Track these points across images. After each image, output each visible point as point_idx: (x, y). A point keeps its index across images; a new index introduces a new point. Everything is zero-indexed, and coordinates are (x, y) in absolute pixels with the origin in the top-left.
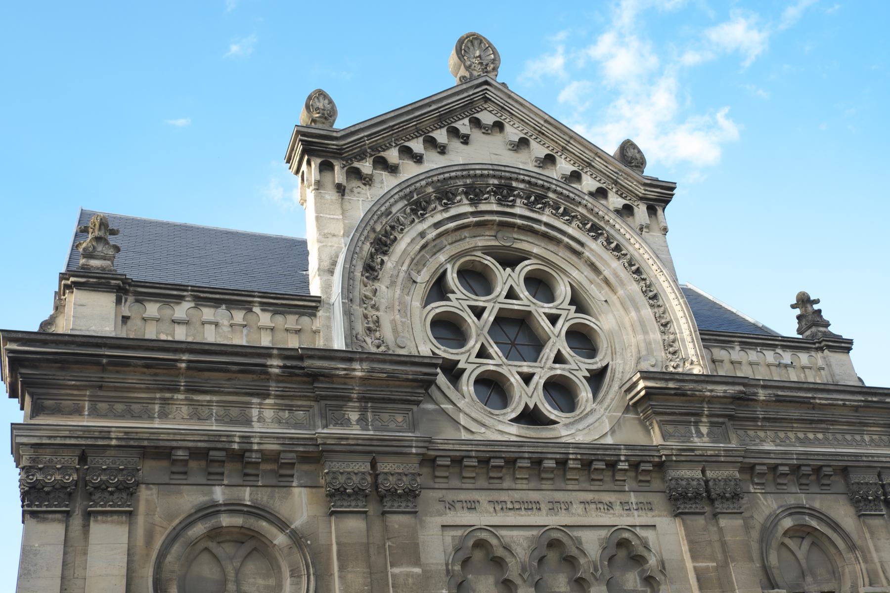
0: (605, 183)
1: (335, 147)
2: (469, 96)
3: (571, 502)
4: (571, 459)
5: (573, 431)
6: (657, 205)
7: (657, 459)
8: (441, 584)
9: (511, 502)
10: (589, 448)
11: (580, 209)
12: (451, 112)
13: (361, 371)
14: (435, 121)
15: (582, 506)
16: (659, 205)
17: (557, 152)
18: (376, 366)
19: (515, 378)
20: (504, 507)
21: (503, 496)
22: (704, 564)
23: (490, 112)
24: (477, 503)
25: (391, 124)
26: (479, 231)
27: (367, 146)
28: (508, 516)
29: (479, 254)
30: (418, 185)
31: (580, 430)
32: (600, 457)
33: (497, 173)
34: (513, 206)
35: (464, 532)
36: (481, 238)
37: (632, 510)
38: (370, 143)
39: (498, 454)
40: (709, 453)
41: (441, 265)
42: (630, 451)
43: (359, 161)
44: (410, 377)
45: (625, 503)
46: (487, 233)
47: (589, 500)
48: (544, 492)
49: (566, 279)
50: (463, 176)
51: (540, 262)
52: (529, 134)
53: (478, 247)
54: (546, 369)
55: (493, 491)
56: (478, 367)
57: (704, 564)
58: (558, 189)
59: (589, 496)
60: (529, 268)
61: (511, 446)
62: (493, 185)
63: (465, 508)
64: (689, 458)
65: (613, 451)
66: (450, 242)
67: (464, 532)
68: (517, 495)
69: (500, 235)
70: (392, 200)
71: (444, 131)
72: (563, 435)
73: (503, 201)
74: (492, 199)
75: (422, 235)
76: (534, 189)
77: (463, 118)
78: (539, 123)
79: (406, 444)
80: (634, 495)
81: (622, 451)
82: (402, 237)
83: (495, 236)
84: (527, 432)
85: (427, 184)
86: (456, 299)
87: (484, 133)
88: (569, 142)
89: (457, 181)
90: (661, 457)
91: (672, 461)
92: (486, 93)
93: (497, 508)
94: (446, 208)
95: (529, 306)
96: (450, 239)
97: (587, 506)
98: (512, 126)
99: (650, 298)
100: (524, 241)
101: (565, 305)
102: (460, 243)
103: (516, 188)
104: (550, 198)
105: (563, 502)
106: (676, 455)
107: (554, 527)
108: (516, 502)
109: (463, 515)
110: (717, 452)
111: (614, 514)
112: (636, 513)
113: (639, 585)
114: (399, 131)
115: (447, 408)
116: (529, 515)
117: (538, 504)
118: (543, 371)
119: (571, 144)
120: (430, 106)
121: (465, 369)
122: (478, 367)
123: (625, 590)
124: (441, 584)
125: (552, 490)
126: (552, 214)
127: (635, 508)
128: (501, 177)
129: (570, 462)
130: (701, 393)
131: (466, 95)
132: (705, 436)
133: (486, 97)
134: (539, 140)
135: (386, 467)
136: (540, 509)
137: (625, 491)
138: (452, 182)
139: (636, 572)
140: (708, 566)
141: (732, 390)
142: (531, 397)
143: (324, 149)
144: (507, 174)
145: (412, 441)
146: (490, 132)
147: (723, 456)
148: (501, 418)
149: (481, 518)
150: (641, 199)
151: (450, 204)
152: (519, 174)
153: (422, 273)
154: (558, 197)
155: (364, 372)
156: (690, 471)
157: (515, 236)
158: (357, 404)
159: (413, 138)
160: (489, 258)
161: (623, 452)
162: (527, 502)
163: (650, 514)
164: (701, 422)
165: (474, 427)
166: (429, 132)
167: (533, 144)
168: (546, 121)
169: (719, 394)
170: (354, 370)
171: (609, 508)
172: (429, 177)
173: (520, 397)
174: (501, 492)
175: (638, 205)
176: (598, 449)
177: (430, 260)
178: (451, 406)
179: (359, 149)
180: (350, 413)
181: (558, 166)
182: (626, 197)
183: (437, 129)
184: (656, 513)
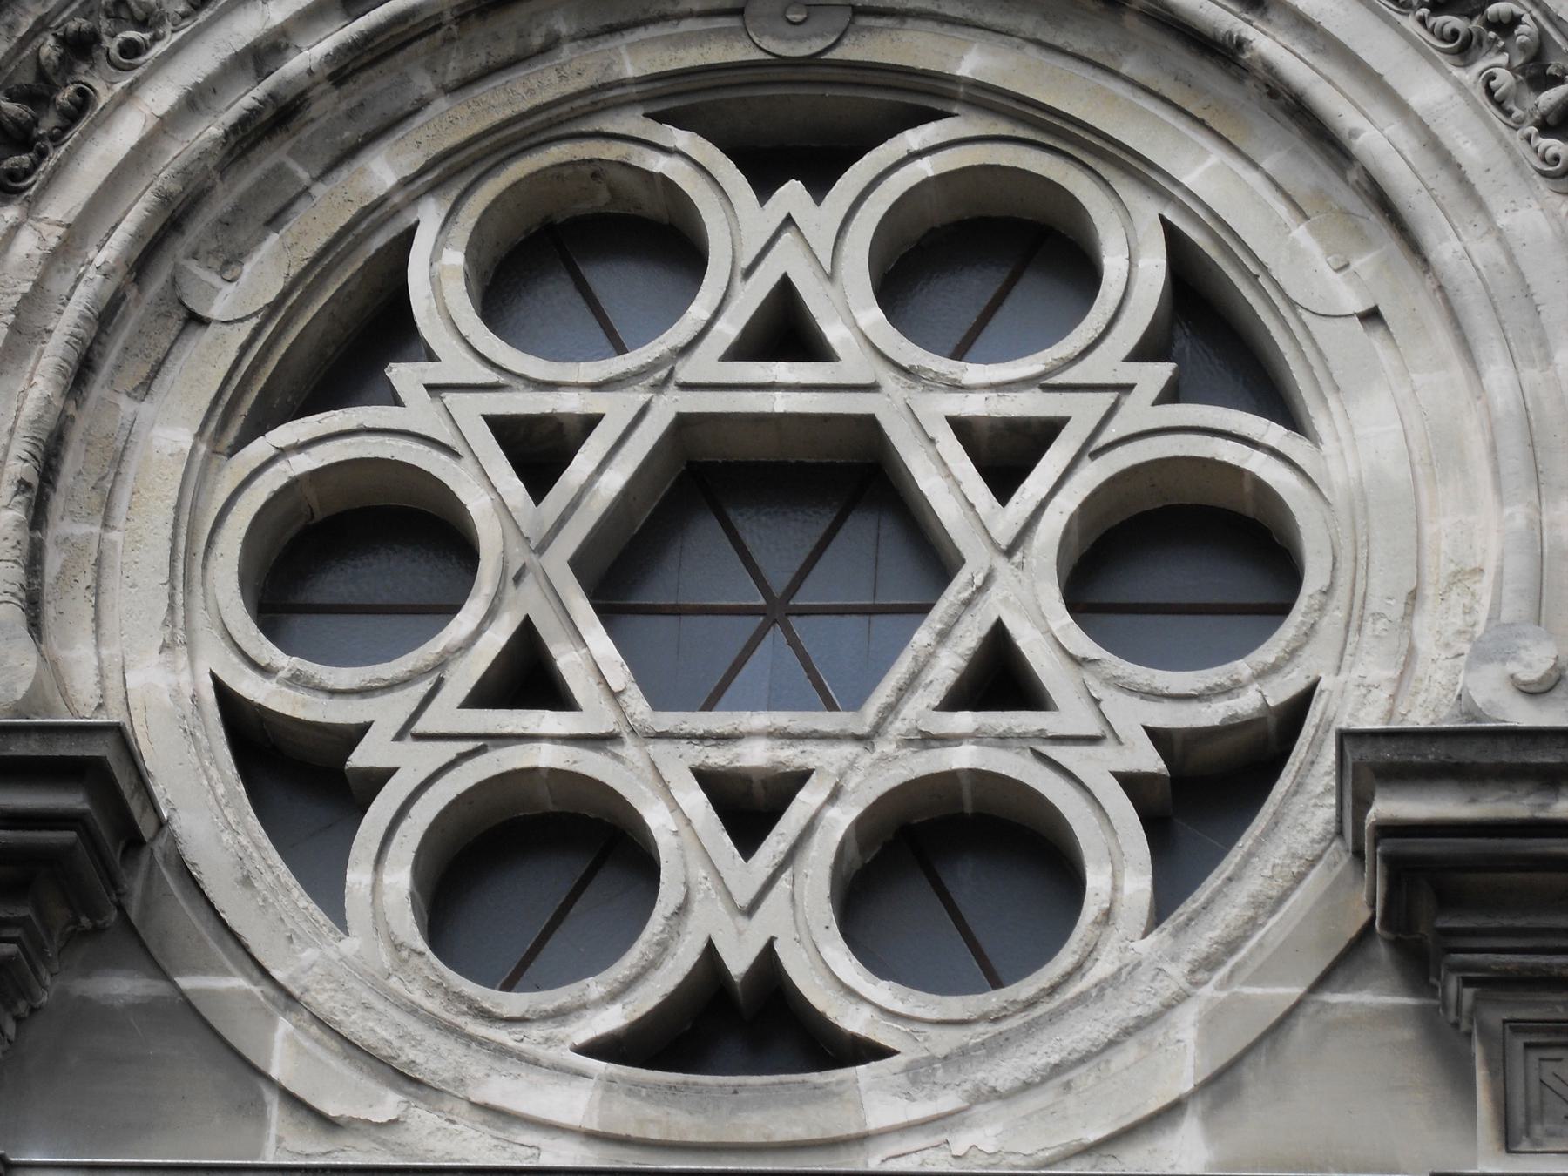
5: (948, 1101)
19: (675, 807)
29: (632, 122)
31: (995, 1095)
41: (376, 211)
49: (1148, 211)
51: (1022, 132)
53: (622, 83)
54: (885, 747)
60: (926, 168)
72: (874, 1122)
82: (130, 91)
84: (651, 1111)
95: (872, 388)
101: (1108, 364)
118: (867, 759)
121: (390, 772)
142: (750, 910)
153: (247, 268)
160: (682, 139)
173: (682, 910)
177: (319, 190)
178: (238, 982)
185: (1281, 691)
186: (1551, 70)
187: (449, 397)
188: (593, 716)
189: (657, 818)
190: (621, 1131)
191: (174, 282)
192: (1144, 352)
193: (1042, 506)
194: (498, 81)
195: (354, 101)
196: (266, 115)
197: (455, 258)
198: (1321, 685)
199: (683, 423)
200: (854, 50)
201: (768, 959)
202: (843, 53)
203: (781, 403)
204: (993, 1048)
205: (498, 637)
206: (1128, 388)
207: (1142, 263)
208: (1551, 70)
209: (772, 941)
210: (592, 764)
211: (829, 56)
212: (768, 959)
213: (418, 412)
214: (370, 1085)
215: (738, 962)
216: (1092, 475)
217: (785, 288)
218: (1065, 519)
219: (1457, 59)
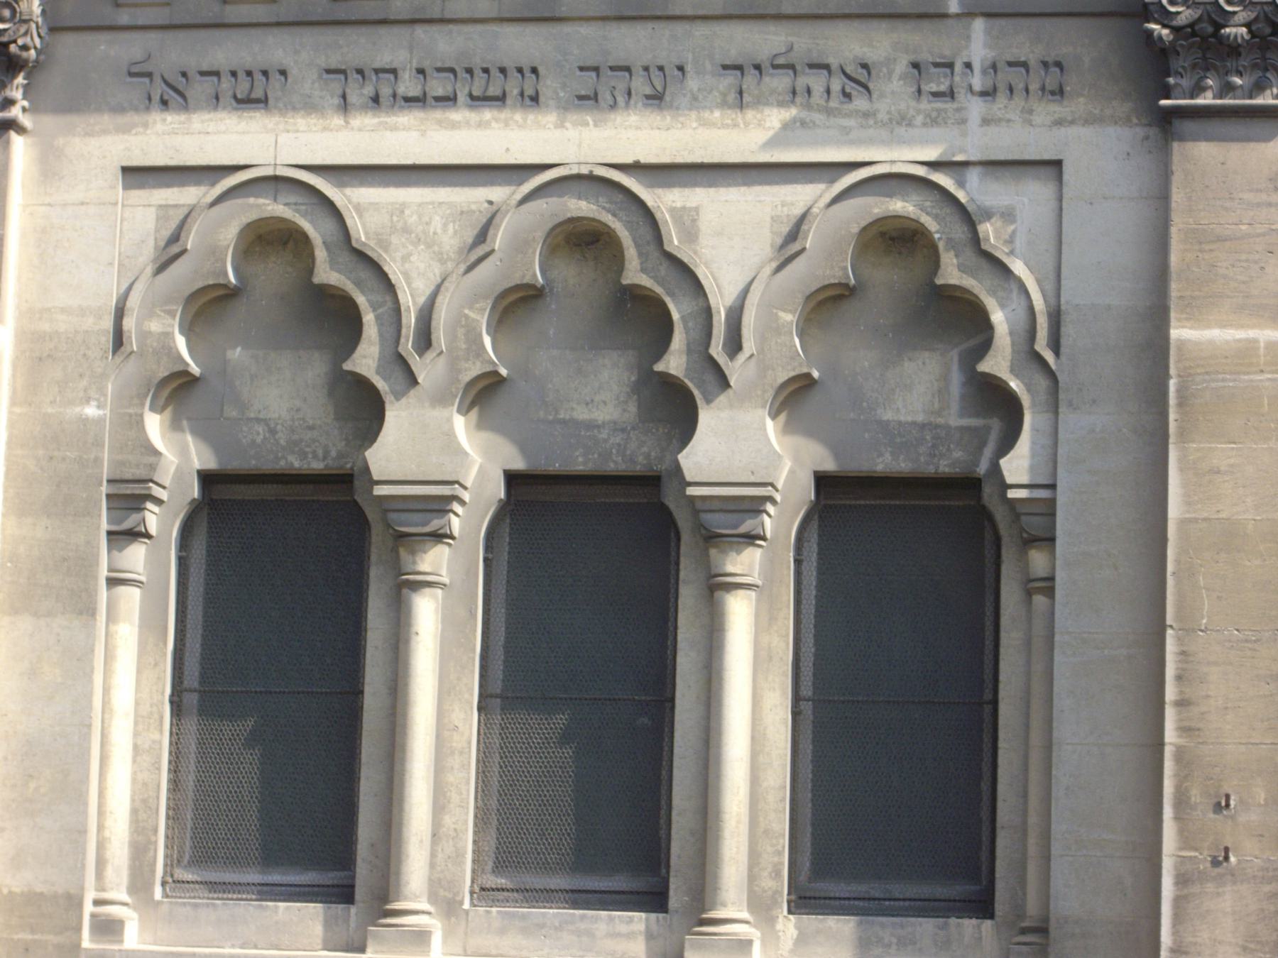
3: (681, 68)
8: (84, 383)
9: (421, 71)
15: (730, 79)
20: (385, 91)
22: (1240, 334)
24: (276, 78)
28: (394, 128)
35: (204, 195)
37: (961, 94)
45: (936, 65)
47: (763, 55)
48: (567, 28)
55: (348, 30)
57: (1240, 334)
63: (226, 98)
67: (204, 195)
80: (988, 32)
93: (353, 98)
97: (750, 80)
105: (646, 69)
107: (584, 170)
108: (439, 70)
109: (211, 127)
111: (866, 115)
112: (976, 108)
113: (955, 406)
116: (481, 125)
117: (530, 77)
123: (880, 422)
124: (84, 383)
125: (604, 19)
127: (977, 86)
136: (535, 99)
137: (944, 16)
139: (954, 355)
140: (1255, 341)
149: (283, 138)
162: (486, 71)
163: (1046, 111)
174: (383, 30)
184: (1078, 105)
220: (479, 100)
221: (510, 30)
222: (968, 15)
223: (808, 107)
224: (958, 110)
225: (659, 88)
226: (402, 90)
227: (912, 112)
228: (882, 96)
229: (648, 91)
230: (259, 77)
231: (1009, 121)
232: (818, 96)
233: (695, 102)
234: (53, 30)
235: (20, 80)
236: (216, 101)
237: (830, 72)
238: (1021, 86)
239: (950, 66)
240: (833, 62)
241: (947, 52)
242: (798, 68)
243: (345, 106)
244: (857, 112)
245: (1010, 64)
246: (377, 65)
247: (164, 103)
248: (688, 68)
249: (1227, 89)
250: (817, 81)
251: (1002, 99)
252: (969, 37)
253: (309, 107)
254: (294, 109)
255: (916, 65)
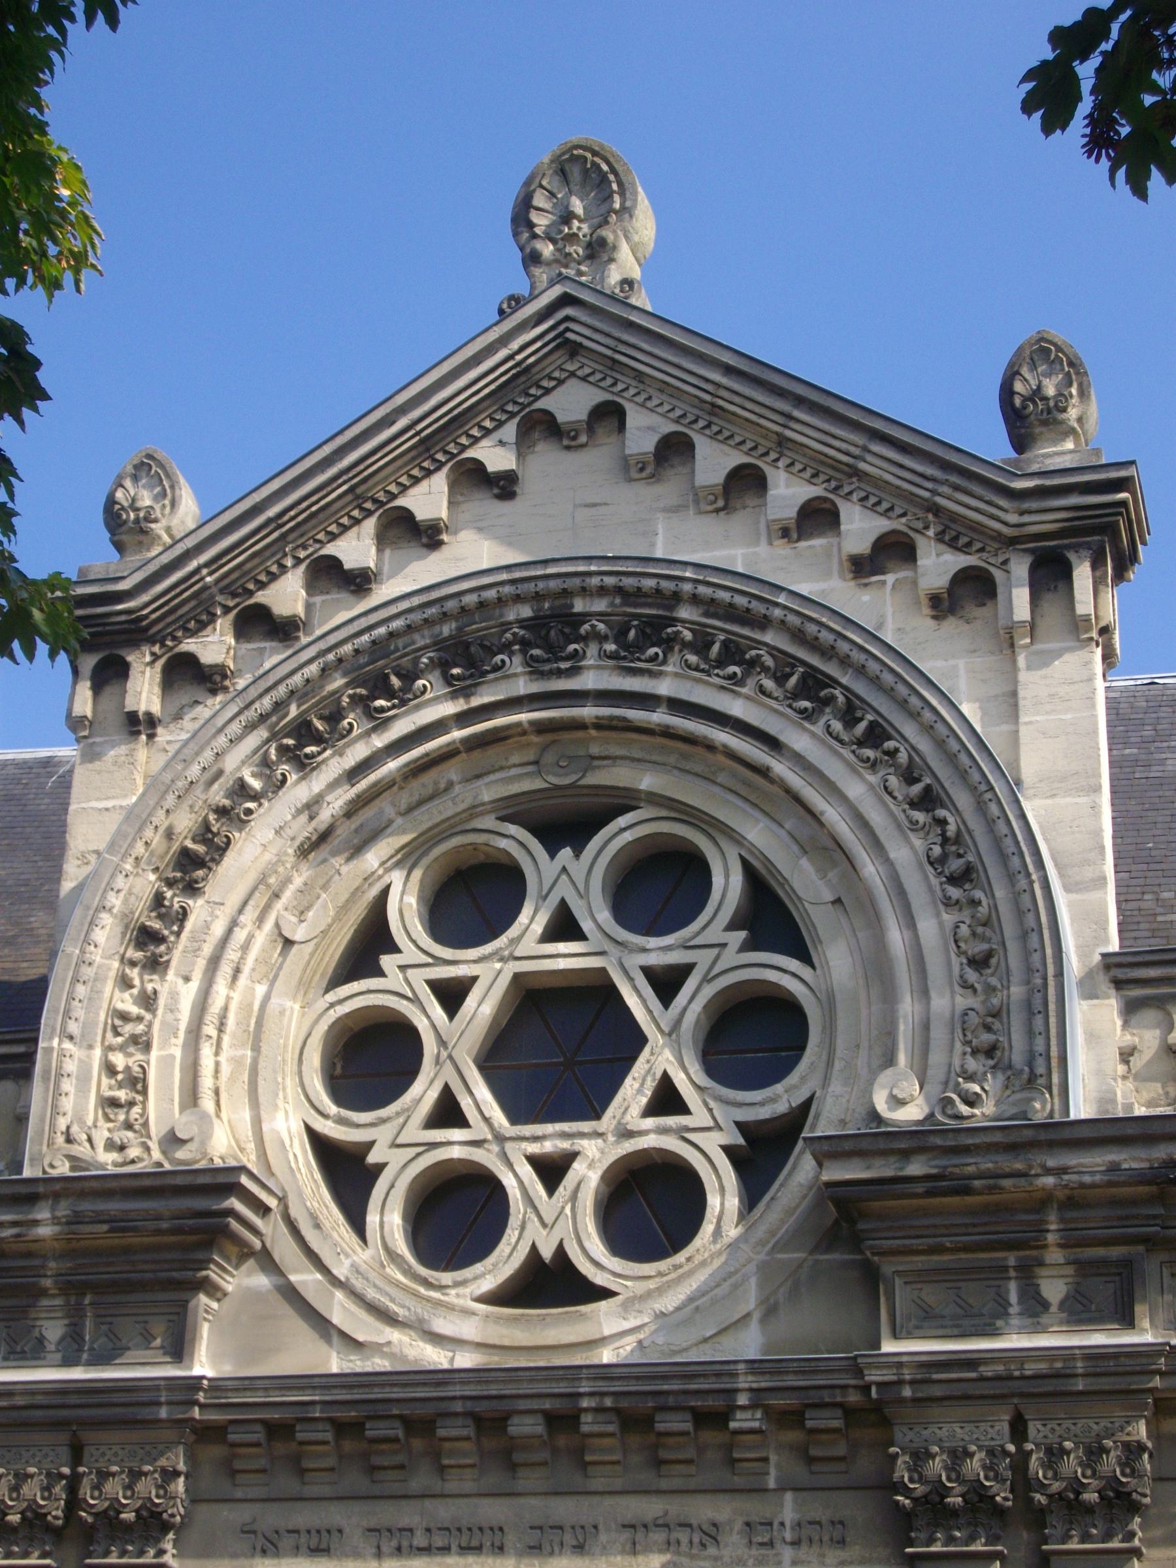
0: (904, 515)
1: (123, 618)
2: (511, 357)
3: (595, 1527)
4: (586, 1410)
6: (1069, 547)
7: (853, 1398)
9: (428, 1530)
10: (637, 1378)
11: (769, 637)
12: (458, 422)
13: (54, 1224)
14: (413, 459)
15: (627, 1535)
16: (1076, 548)
17: (766, 454)
18: (86, 1206)
20: (405, 1544)
21: (408, 1515)
23: (584, 379)
24: (335, 1534)
25: (272, 512)
26: (492, 754)
27: (214, 590)
29: (489, 822)
30: (297, 679)
32: (671, 1401)
33: (524, 588)
34: (575, 671)
36: (492, 777)
37: (778, 1544)
38: (218, 581)
39: (381, 1409)
40: (1030, 1368)
41: (369, 878)
42: (767, 1377)
43: (193, 633)
44: (165, 1225)
45: (762, 1524)
46: (515, 759)
48: (522, 1501)
50: (426, 620)
51: (673, 815)
52: (690, 418)
53: (483, 804)
56: (418, 1155)
58: (702, 590)
59: (651, 1508)
60: (628, 836)
61: (417, 1385)
62: (521, 622)
63: (304, 1549)
64: (957, 1390)
65: (713, 1379)
66: (403, 807)
68: (444, 1511)
69: (549, 758)
70: (222, 740)
71: (439, 482)
72: (607, 1332)
73: (548, 660)
74: (516, 664)
75: (311, 807)
76: (636, 606)
77: (500, 424)
78: (707, 380)
79: (144, 1397)
80: (795, 1501)
81: (741, 1379)
83: (536, 763)
84: (504, 1331)
85: (323, 670)
86: (400, 967)
87: (568, 448)
88: (790, 417)
89: (416, 636)
90: (866, 1388)
91: (902, 1401)
92: (567, 330)
93: (384, 1549)
94: (382, 725)
96: (405, 799)
97: (640, 1536)
98: (643, 405)
99: (953, 880)
100: (622, 758)
101: (715, 933)
102: (436, 802)
103: (584, 617)
104: (683, 621)
105: (573, 1527)
106: (912, 1382)
108: (440, 1529)
110: (1059, 1365)
111: (716, 1559)
112: (787, 1553)
114: (299, 525)
115: (304, 1282)
119: (798, 421)
120: (394, 422)
121: (384, 1165)
122: (418, 1155)
125: (546, 1494)
126: (689, 667)
128: (538, 597)
129: (586, 1418)
130: (1022, 1182)
131: (503, 353)
132: (1054, 1309)
133: (567, 341)
134: (715, 429)
135: (103, 1454)
138: (400, 642)
141: (1142, 1160)
143: (99, 629)
144: (553, 584)
145: (157, 1388)
146: (583, 439)
147: (1083, 1375)
148: (452, 1296)
150: (1012, 542)
151: (394, 707)
152: (589, 574)
154: (706, 614)
155: (58, 1224)
156: (969, 1427)
157: (595, 750)
158: (58, 1302)
159: (345, 529)
160: (513, 829)
161: (744, 1382)
162: (470, 1529)
164: (1041, 1264)
165: (364, 1328)
166: (394, 497)
167: (704, 447)
168: (729, 370)
169: (1087, 1179)
170: (36, 1223)
171: (706, 1539)
172: (329, 650)
174: (404, 1502)
175: (1005, 562)
176: (665, 1378)
178: (319, 1276)
179: (193, 603)
180: (45, 1323)
181: (772, 492)
182: (969, 544)
183: (416, 481)
185: (797, 1099)
186: (915, 775)
187: (410, 973)
188: (479, 1131)
189: (509, 1181)
190: (491, 1341)
191: (277, 925)
192: (732, 927)
193: (685, 1009)
194: (424, 808)
195: (358, 823)
196: (314, 838)
197: (412, 900)
198: (817, 1095)
199: (517, 977)
200: (592, 779)
201: (560, 1252)
202: (583, 782)
203: (562, 964)
204: (660, 1291)
205: (433, 1094)
206: (724, 945)
207: (731, 879)
208: (915, 775)
209: (562, 1240)
210: (478, 1155)
211: (580, 783)
212: (560, 1252)
213: (394, 979)
214: (379, 1325)
215: (547, 1253)
216: (709, 991)
217: (563, 903)
218: (695, 1015)
219: (870, 771)
220: (465, 1550)
221: (486, 1501)
222: (781, 1489)
223: (678, 1553)
224: (776, 1555)
225: (581, 1541)
226: (415, 1543)
227: (746, 1557)
228: (726, 1545)
229: (575, 1543)
230: (325, 1534)
231: (809, 1562)
232: (684, 1547)
233: (605, 1551)
234: (194, 1501)
235: (171, 1536)
236: (296, 1551)
237: (692, 1530)
238: (817, 1538)
239: (771, 1524)
240: (694, 1522)
241: (768, 1515)
242: (672, 1526)
243: (379, 1555)
244: (710, 1556)
245: (810, 1523)
246: (400, 1526)
247: (264, 1552)
248: (600, 1527)
249: (951, 1540)
250: (683, 1536)
251: (804, 1548)
252: (782, 1506)
253: (356, 1554)
254: (347, 1556)
255: (748, 1524)
